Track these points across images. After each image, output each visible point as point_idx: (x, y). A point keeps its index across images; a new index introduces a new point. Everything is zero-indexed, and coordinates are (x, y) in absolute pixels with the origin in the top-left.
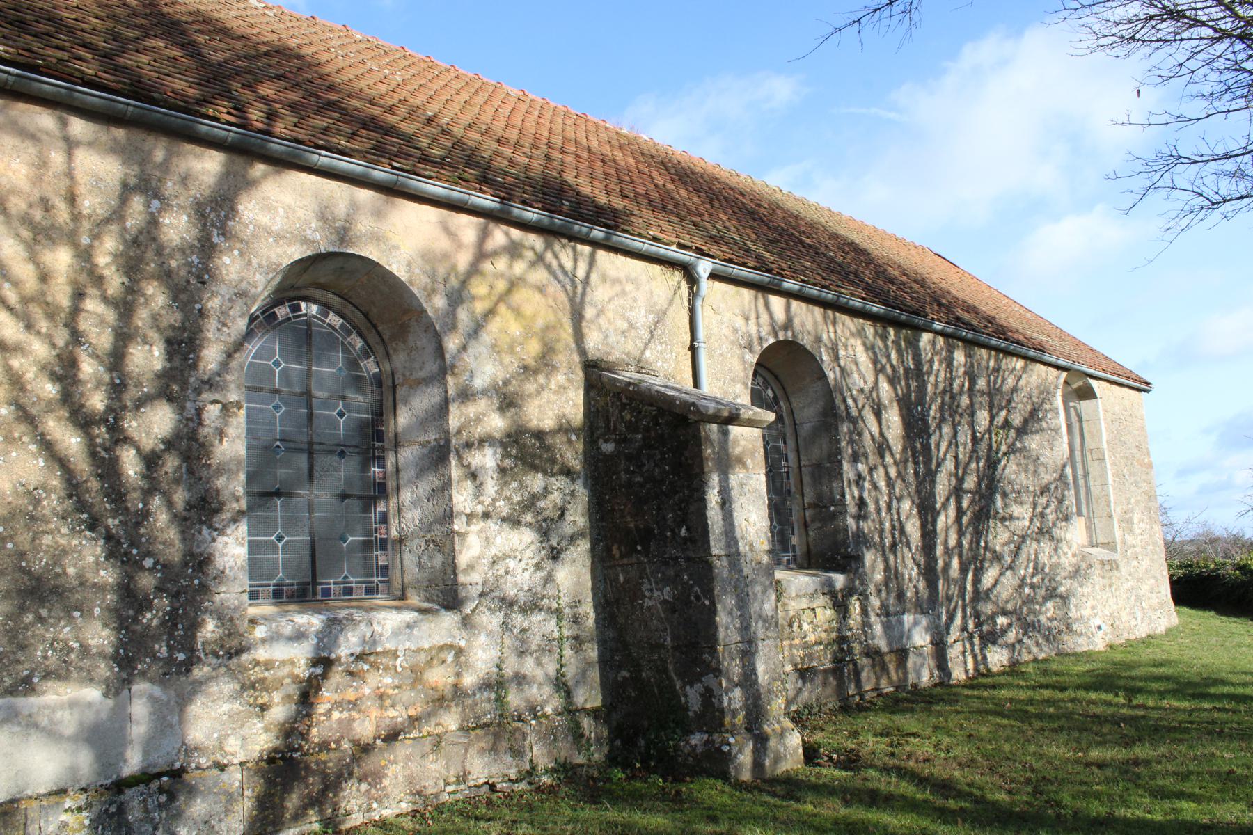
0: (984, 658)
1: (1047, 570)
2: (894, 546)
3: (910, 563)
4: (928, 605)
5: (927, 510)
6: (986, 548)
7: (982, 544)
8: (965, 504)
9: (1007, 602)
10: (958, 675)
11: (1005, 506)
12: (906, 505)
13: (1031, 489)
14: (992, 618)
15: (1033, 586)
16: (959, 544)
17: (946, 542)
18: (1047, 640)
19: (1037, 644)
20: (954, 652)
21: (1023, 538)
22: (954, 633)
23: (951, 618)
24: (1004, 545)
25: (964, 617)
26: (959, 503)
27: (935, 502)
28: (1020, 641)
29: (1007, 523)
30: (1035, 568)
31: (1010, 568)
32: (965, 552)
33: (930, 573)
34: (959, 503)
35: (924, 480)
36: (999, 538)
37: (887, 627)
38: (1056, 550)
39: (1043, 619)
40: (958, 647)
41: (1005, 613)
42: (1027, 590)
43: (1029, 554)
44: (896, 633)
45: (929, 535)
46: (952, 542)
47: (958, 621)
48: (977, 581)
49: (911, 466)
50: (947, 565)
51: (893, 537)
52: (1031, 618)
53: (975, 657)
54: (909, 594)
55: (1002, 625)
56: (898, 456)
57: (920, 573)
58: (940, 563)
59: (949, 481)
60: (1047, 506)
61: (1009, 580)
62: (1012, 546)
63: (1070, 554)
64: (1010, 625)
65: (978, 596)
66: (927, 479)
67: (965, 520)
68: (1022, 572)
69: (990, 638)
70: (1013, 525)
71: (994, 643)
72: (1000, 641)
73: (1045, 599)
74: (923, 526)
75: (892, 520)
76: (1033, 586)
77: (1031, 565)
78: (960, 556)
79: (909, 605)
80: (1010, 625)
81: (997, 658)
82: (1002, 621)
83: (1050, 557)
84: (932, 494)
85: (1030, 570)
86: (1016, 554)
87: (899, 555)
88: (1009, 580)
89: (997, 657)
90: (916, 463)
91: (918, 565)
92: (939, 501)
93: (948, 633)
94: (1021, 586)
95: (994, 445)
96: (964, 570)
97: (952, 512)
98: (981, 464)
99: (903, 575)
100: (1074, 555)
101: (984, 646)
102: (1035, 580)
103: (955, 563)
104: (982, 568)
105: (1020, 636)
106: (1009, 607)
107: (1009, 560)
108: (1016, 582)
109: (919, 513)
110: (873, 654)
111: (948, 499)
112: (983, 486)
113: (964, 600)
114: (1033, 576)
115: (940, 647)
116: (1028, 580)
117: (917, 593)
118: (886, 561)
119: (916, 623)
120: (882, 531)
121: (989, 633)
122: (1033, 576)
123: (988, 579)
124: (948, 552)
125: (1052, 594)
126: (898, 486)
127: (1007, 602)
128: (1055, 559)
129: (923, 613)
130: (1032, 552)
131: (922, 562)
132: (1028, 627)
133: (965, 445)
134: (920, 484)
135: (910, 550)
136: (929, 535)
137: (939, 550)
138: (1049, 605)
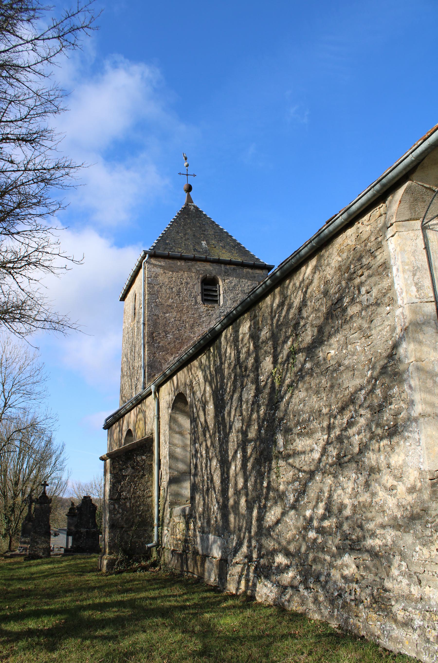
0: (255, 585)
1: (348, 512)
2: (208, 490)
3: (214, 501)
4: (223, 530)
5: (225, 464)
6: (269, 487)
7: (265, 484)
8: (249, 451)
9: (289, 542)
10: (231, 588)
11: (286, 443)
12: (214, 462)
13: (325, 411)
14: (273, 553)
15: (321, 531)
16: (245, 486)
17: (236, 484)
18: (332, 602)
19: (316, 601)
20: (235, 570)
21: (312, 474)
22: (239, 558)
23: (240, 544)
24: (288, 483)
25: (249, 547)
26: (244, 451)
27: (228, 457)
28: (295, 588)
29: (291, 461)
30: (328, 509)
31: (293, 507)
32: (250, 493)
33: (224, 509)
34: (244, 451)
35: (223, 443)
36: (283, 476)
37: (202, 539)
38: (367, 485)
39: (336, 575)
40: (238, 568)
41: (288, 554)
42: (312, 534)
43: (321, 491)
44: (206, 545)
45: (225, 480)
46: (241, 484)
47: (244, 549)
48: (261, 519)
49: (217, 434)
50: (237, 503)
51: (208, 485)
52: (316, 567)
53: (247, 581)
54: (212, 522)
55: (280, 564)
56: (211, 432)
57: (218, 508)
58: (231, 502)
59: (237, 437)
60: (350, 424)
61: (292, 521)
62: (297, 483)
63: (401, 488)
64: (287, 567)
65: (264, 532)
66: (224, 442)
67: (249, 465)
68: (308, 513)
69: (265, 571)
70: (297, 462)
71: (267, 577)
72: (274, 578)
73: (342, 550)
74: (222, 475)
75: (207, 474)
76: (321, 531)
77: (322, 505)
78: (247, 495)
79: (212, 529)
80: (287, 567)
81: (265, 591)
82: (280, 559)
83: (356, 495)
84: (227, 452)
85: (321, 511)
86: (302, 492)
87: (210, 496)
88: (292, 521)
89: (265, 590)
90: (219, 432)
91: (218, 503)
92: (231, 453)
93: (234, 555)
94: (306, 529)
95: (277, 384)
96: (250, 509)
97: (239, 462)
98: (262, 412)
99: (211, 508)
100: (412, 490)
101: (258, 575)
102: (326, 524)
103: (243, 501)
104: (265, 506)
105: (296, 583)
106: (292, 548)
107: (291, 498)
108: (301, 522)
109: (221, 467)
110: (196, 553)
111: (236, 452)
112: (263, 431)
113: (250, 532)
114: (324, 518)
115: (224, 565)
116: (315, 523)
117: (216, 521)
118: (204, 500)
119: (215, 542)
120: (203, 481)
121: (264, 566)
122: (324, 518)
123: (271, 516)
124: (237, 493)
125: (352, 546)
126: (211, 450)
127: (289, 542)
128: (365, 498)
129: (219, 536)
130: (326, 489)
131: (221, 500)
132: (308, 575)
133: (247, 402)
134: (221, 445)
135: (215, 492)
136: (225, 480)
137: (231, 491)
138: (347, 558)
